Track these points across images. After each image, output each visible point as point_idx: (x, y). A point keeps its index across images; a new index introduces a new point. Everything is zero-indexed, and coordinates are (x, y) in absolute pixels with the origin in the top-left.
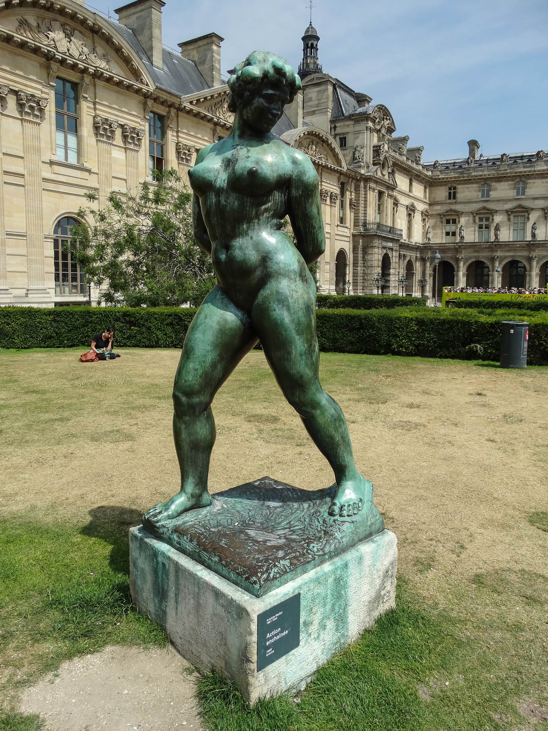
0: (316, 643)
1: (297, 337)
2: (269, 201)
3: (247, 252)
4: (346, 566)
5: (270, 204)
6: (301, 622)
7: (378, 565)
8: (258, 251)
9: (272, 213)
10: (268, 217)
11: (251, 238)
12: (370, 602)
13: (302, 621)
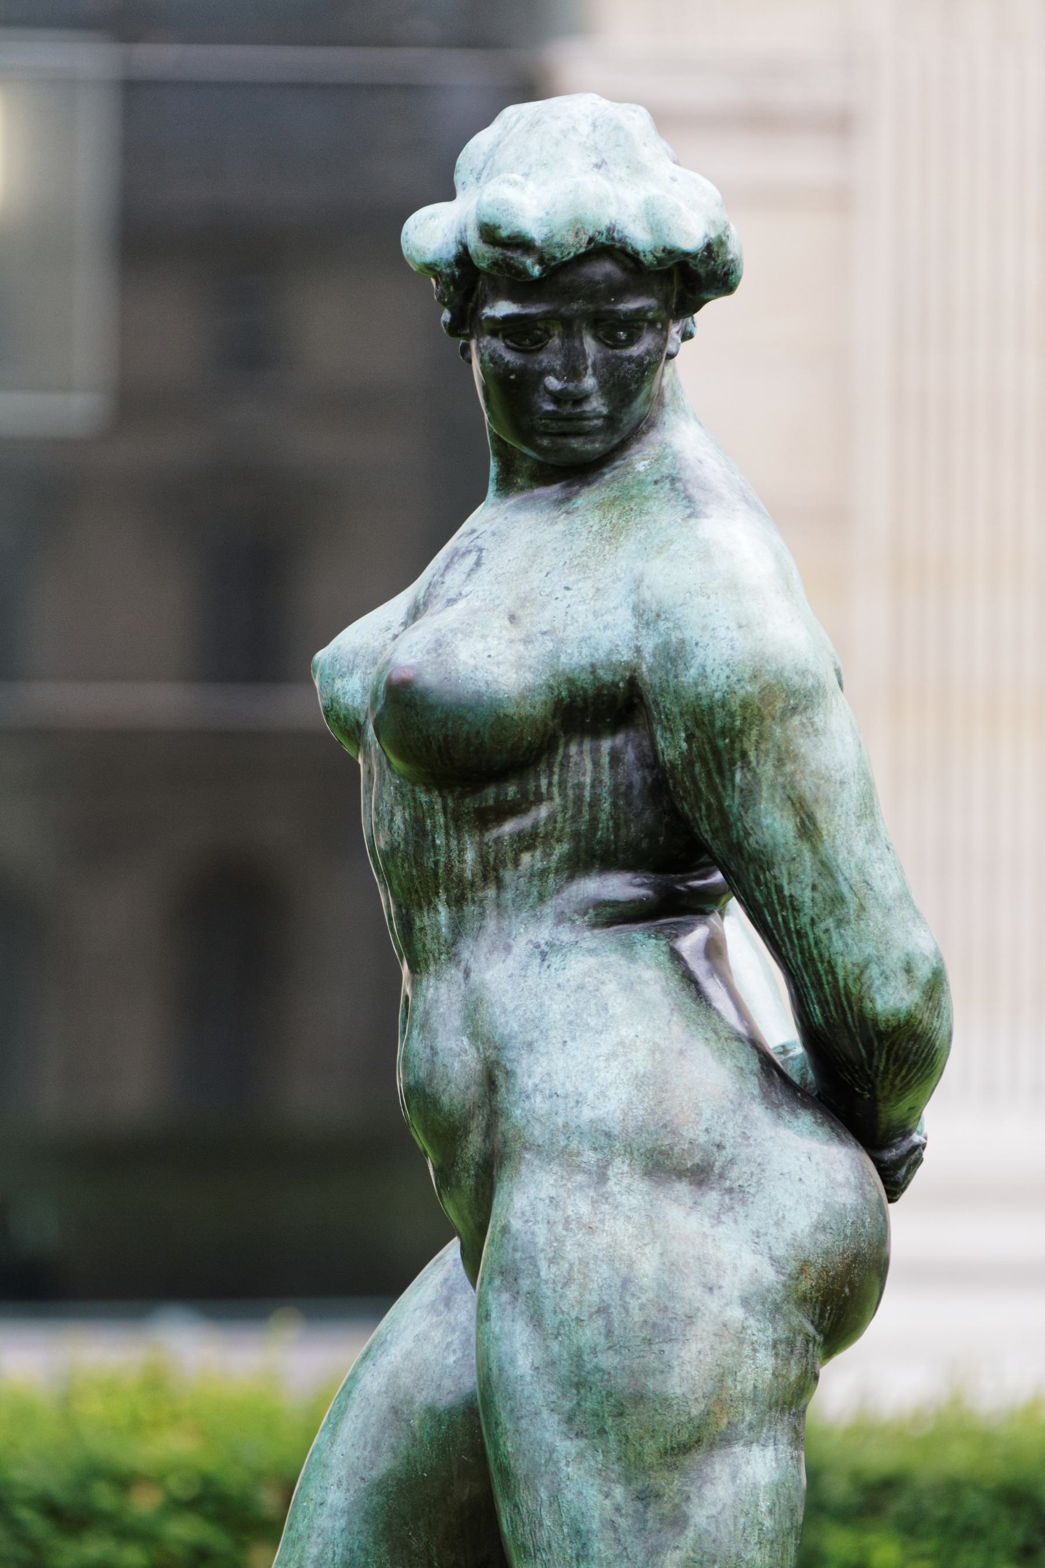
1: (566, 1447)
2: (539, 799)
5: (543, 811)
9: (561, 849)
10: (543, 873)
11: (467, 973)
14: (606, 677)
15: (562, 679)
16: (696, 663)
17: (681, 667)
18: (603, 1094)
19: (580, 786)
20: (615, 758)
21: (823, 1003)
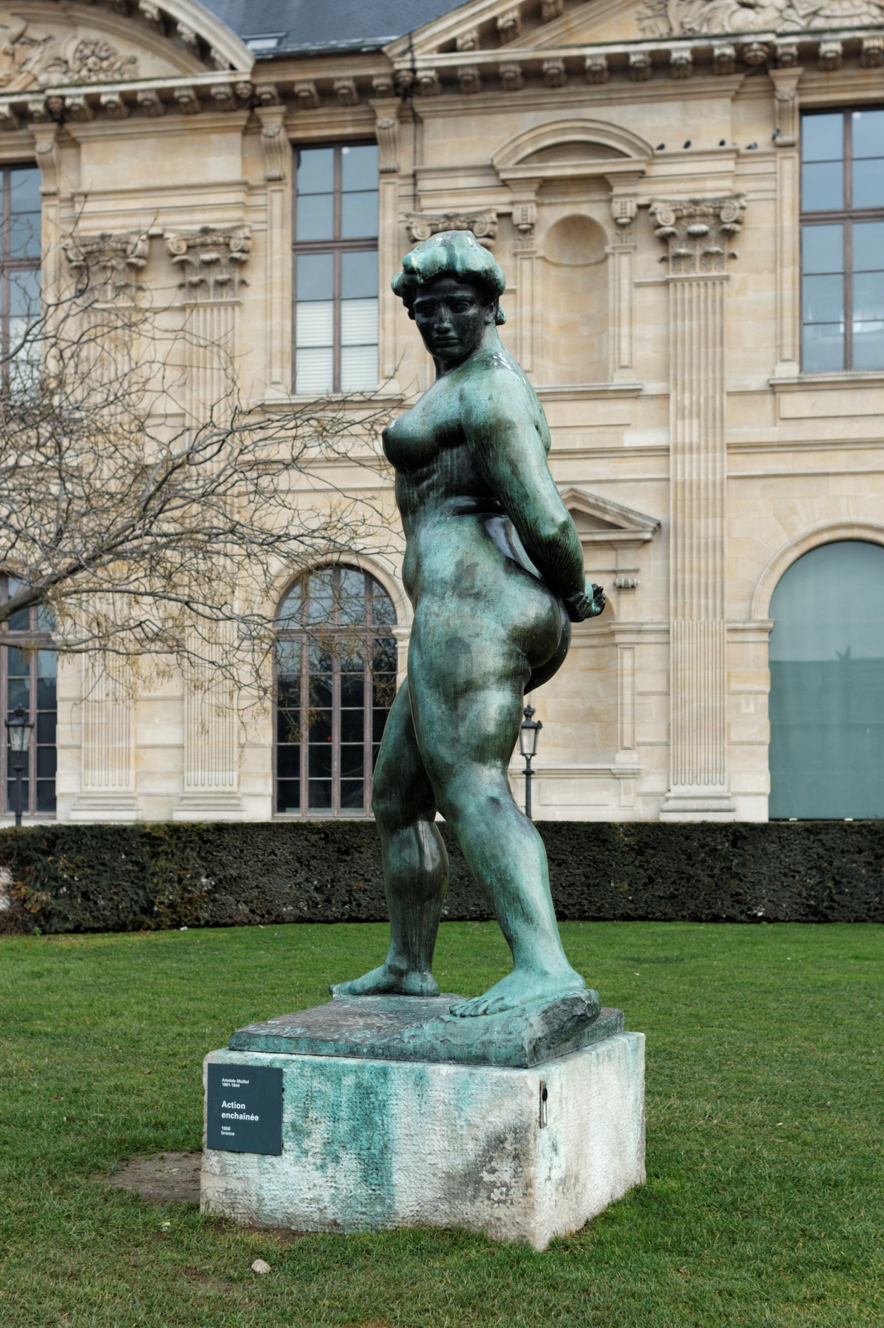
0: (316, 1173)
1: (426, 691)
2: (434, 472)
4: (385, 1074)
5: (435, 477)
6: (285, 1120)
7: (470, 1112)
9: (442, 489)
10: (437, 498)
12: (450, 1176)
13: (287, 1118)
14: (451, 425)
18: (444, 569)
19: (447, 466)
20: (458, 456)
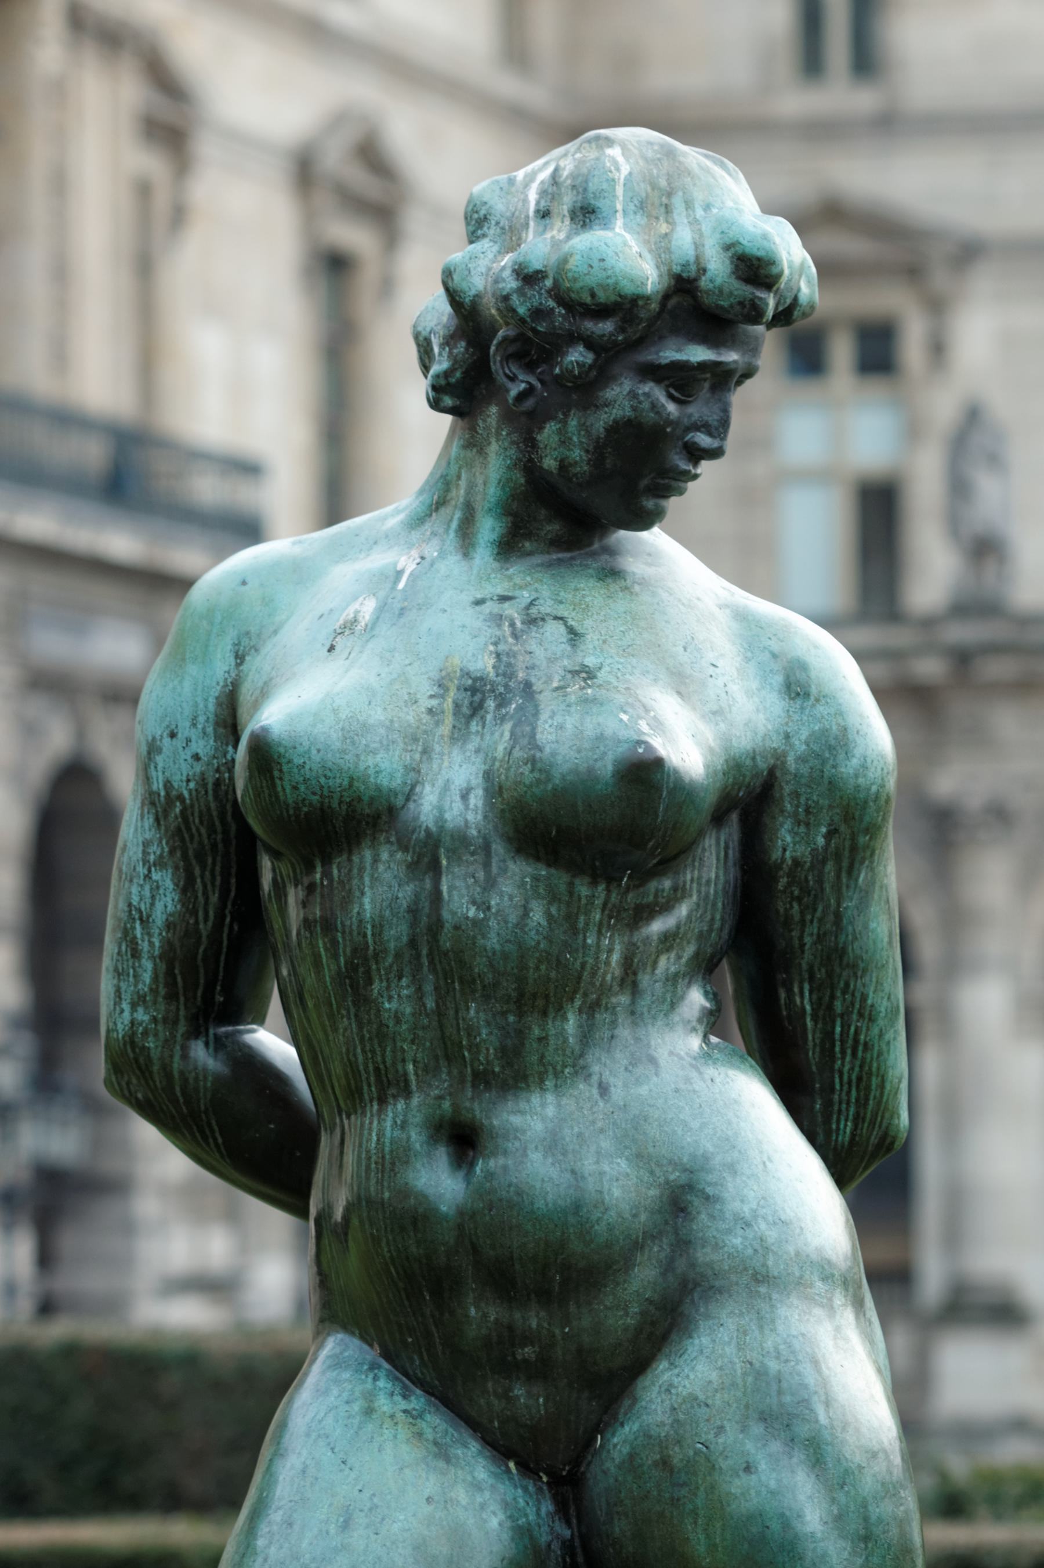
3: (588, 1165)
5: (683, 910)
8: (640, 1157)
11: (604, 1090)
15: (731, 763)
16: (858, 752)
17: (841, 756)
21: (858, 1119)
